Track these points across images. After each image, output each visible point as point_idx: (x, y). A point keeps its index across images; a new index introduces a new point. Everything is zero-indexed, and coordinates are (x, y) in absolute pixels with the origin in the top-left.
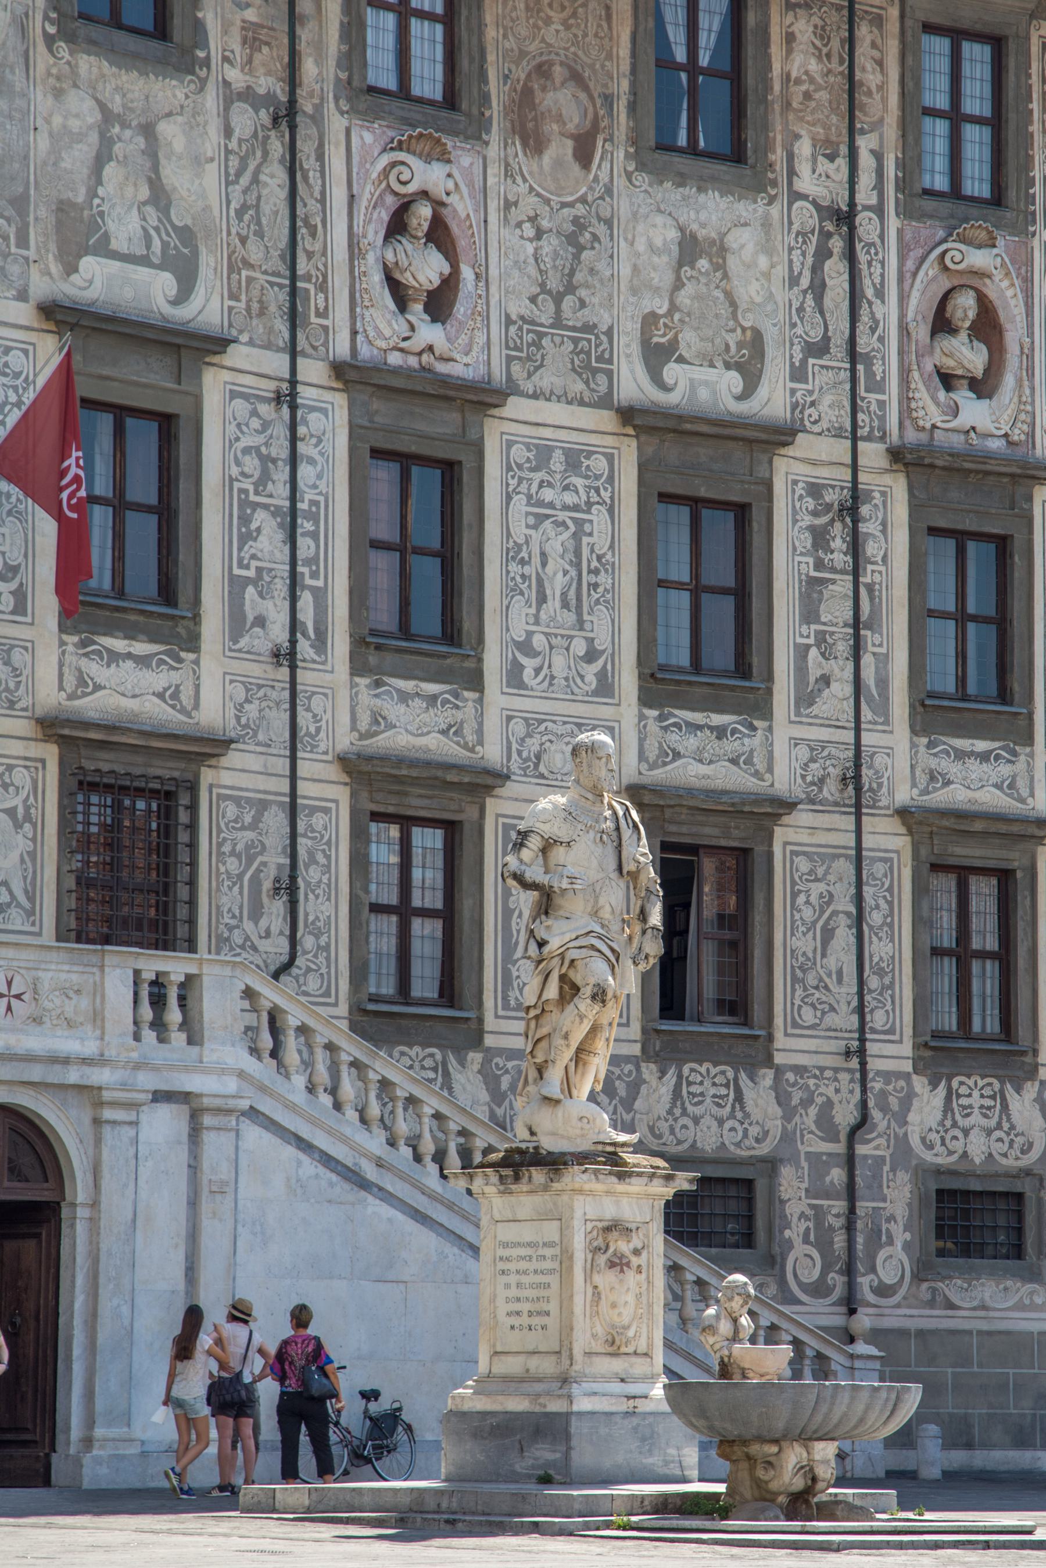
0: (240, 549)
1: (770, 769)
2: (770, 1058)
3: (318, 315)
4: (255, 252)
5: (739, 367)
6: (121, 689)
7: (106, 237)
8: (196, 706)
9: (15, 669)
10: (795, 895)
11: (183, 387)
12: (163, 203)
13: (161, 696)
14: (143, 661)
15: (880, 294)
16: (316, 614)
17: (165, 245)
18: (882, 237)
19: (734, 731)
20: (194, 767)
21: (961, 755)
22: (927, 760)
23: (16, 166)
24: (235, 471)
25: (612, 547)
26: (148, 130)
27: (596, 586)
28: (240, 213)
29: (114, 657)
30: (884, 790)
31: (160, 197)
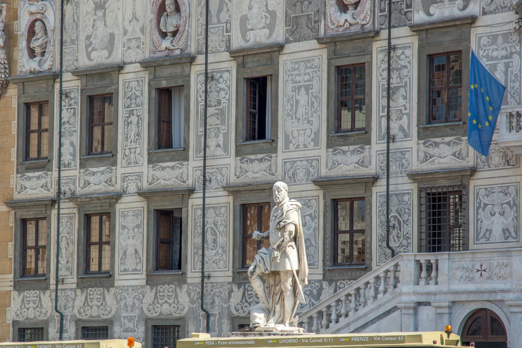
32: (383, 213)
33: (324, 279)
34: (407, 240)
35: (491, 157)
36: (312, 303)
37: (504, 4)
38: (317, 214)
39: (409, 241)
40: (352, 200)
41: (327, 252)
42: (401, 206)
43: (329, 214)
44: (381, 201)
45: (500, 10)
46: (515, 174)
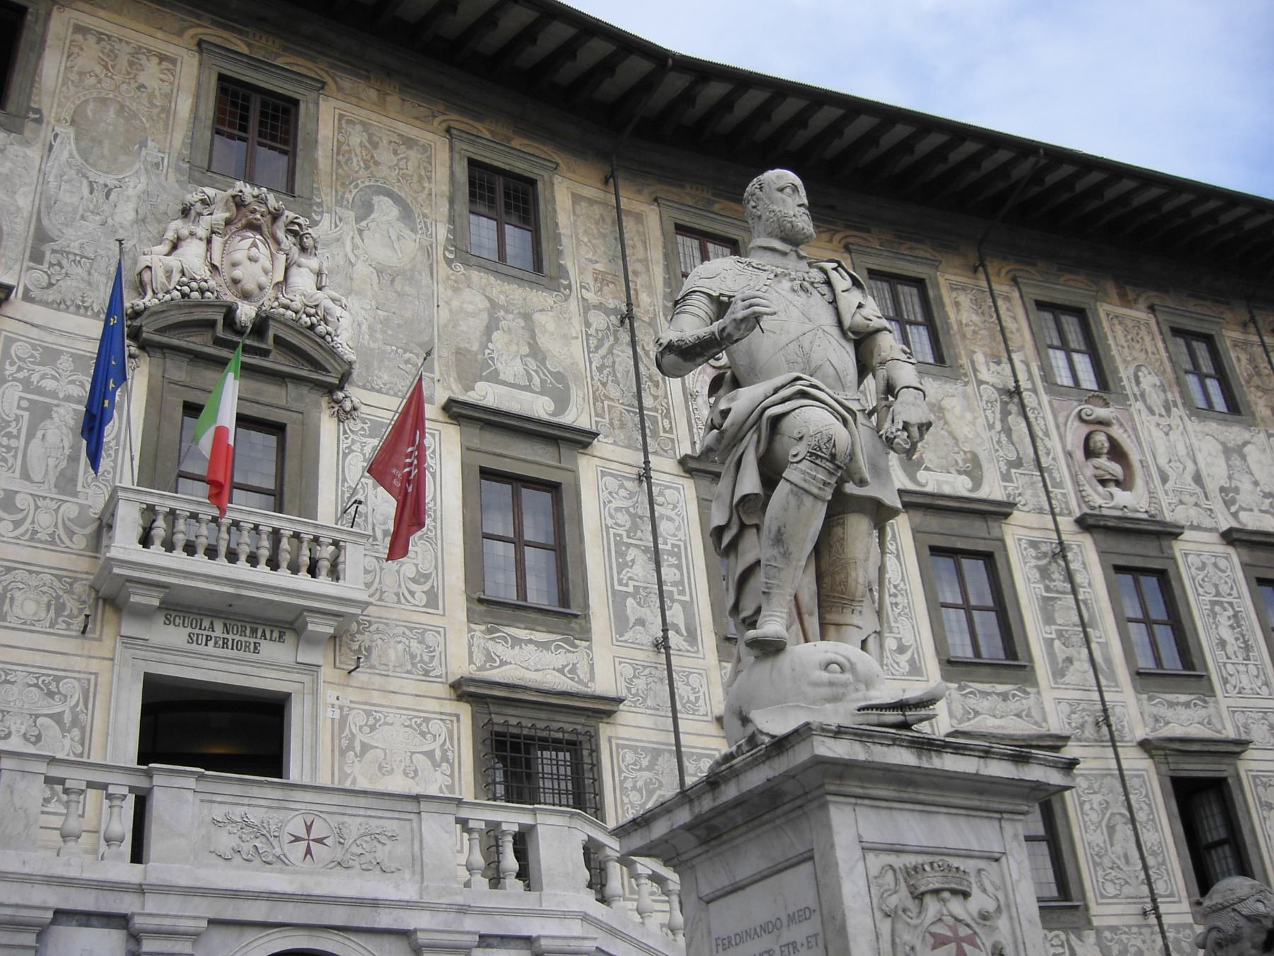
0: (619, 573)
1: (1045, 720)
2: (1089, 922)
3: (665, 431)
4: (613, 391)
5: (966, 473)
6: (525, 665)
7: (496, 372)
8: (592, 679)
9: (428, 647)
10: (1082, 804)
11: (563, 465)
12: (540, 357)
13: (561, 671)
14: (543, 646)
15: (1047, 434)
16: (686, 620)
17: (543, 382)
18: (1039, 404)
19: (1014, 696)
20: (592, 722)
21: (1172, 705)
22: (1150, 709)
23: (423, 325)
24: (610, 522)
25: (903, 579)
26: (527, 317)
27: (896, 604)
28: (600, 369)
29: (517, 642)
30: (1126, 729)
31: (536, 352)
35: (12, 599)
37: (83, 302)
45: (72, 309)
46: (86, 653)
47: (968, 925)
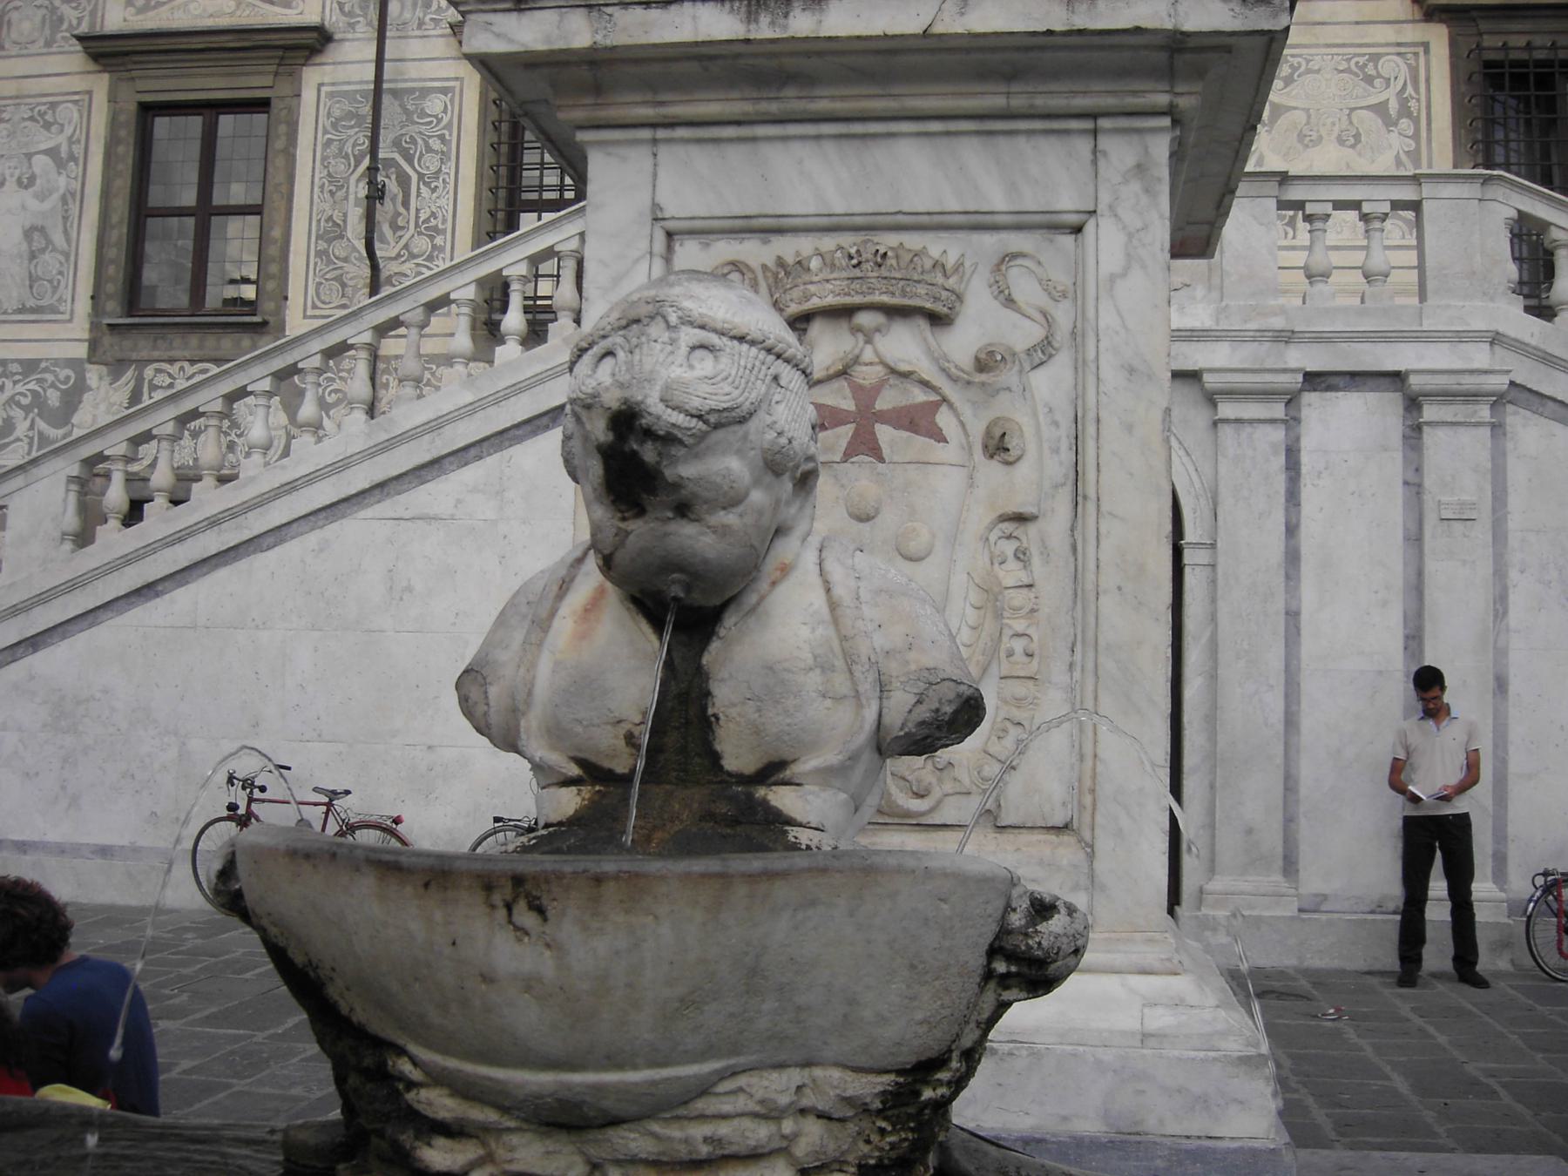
32: (341, 150)
33: (91, 359)
34: (432, 238)
36: (40, 434)
38: (78, 150)
39: (439, 241)
40: (212, 108)
41: (111, 270)
42: (416, 128)
43: (127, 152)
44: (337, 113)
47: (925, 384)
